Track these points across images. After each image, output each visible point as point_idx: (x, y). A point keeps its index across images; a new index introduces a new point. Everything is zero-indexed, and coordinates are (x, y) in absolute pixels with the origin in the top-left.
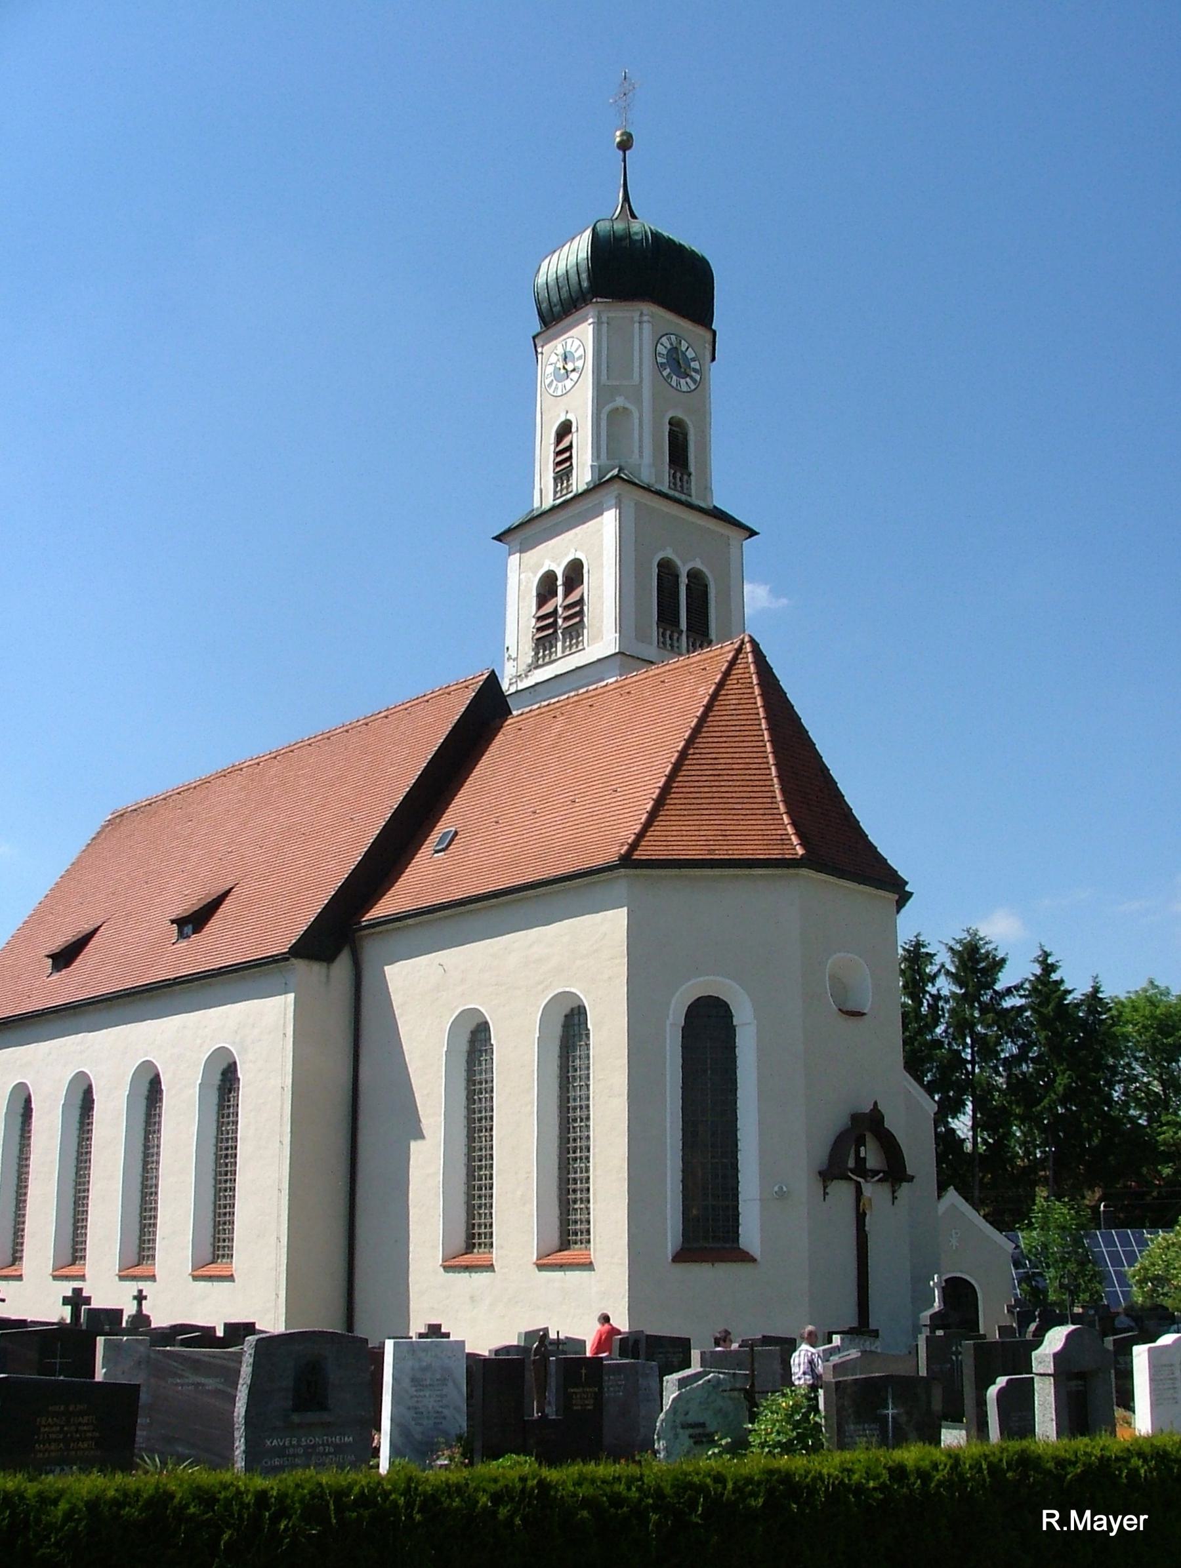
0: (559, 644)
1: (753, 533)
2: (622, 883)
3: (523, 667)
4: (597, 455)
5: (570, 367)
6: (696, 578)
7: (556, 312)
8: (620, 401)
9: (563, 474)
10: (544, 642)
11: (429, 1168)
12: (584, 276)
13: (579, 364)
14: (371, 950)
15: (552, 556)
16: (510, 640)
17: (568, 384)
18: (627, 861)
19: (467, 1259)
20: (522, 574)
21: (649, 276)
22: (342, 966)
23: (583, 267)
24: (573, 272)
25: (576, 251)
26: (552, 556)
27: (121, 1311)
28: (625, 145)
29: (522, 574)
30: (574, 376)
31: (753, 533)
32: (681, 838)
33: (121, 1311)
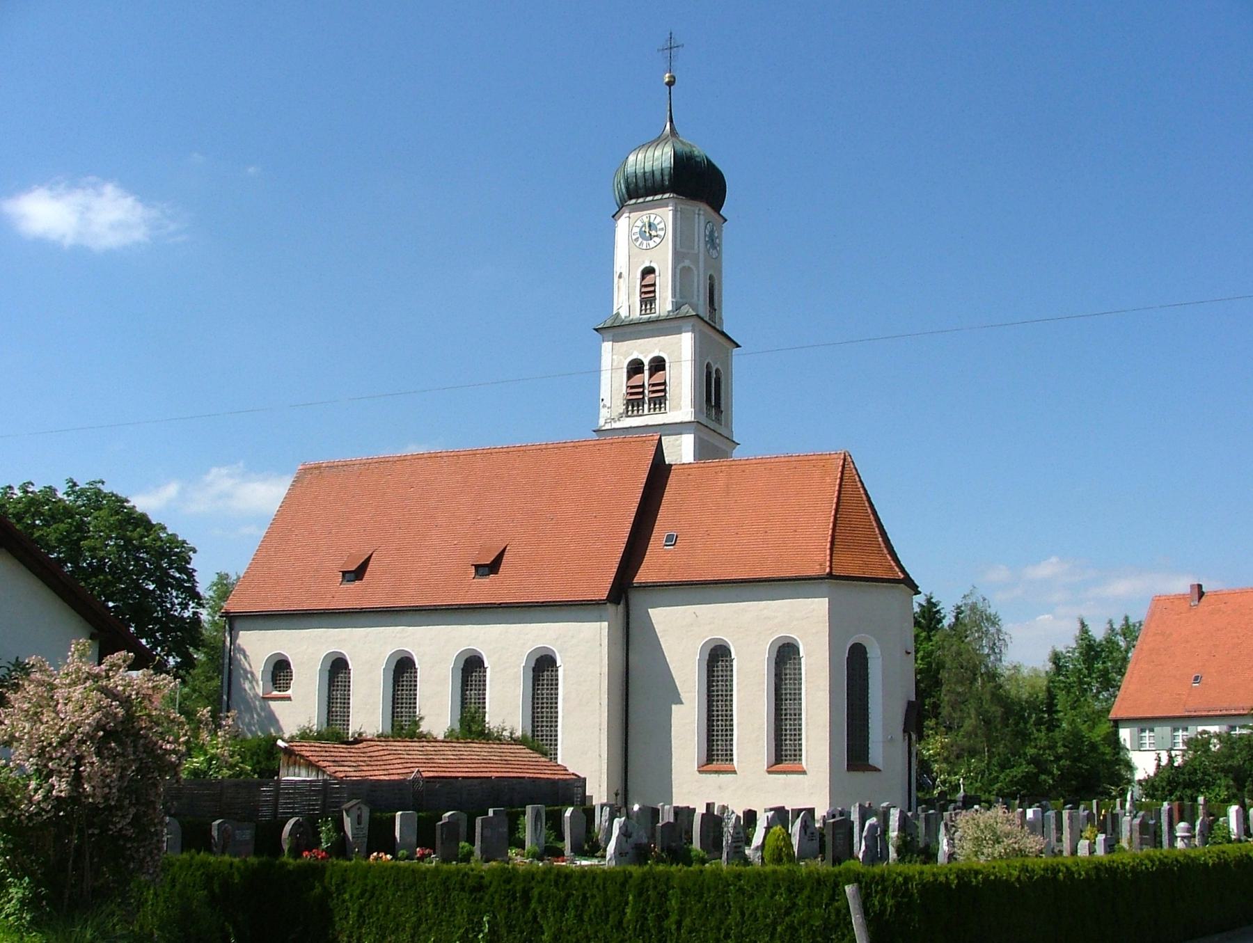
0: (646, 406)
1: (738, 346)
2: (825, 586)
3: (615, 415)
4: (674, 295)
5: (653, 233)
6: (717, 370)
7: (640, 190)
8: (687, 263)
9: (648, 298)
10: (634, 402)
11: (686, 722)
12: (666, 178)
13: (661, 233)
14: (636, 598)
15: (645, 349)
16: (605, 393)
17: (652, 244)
18: (830, 576)
19: (710, 767)
20: (614, 358)
21: (695, 182)
22: (621, 607)
23: (666, 172)
24: (658, 174)
25: (660, 158)
26: (645, 349)
27: (694, 810)
28: (670, 84)
29: (614, 358)
30: (657, 240)
31: (738, 346)
32: (850, 564)
33: (694, 810)
